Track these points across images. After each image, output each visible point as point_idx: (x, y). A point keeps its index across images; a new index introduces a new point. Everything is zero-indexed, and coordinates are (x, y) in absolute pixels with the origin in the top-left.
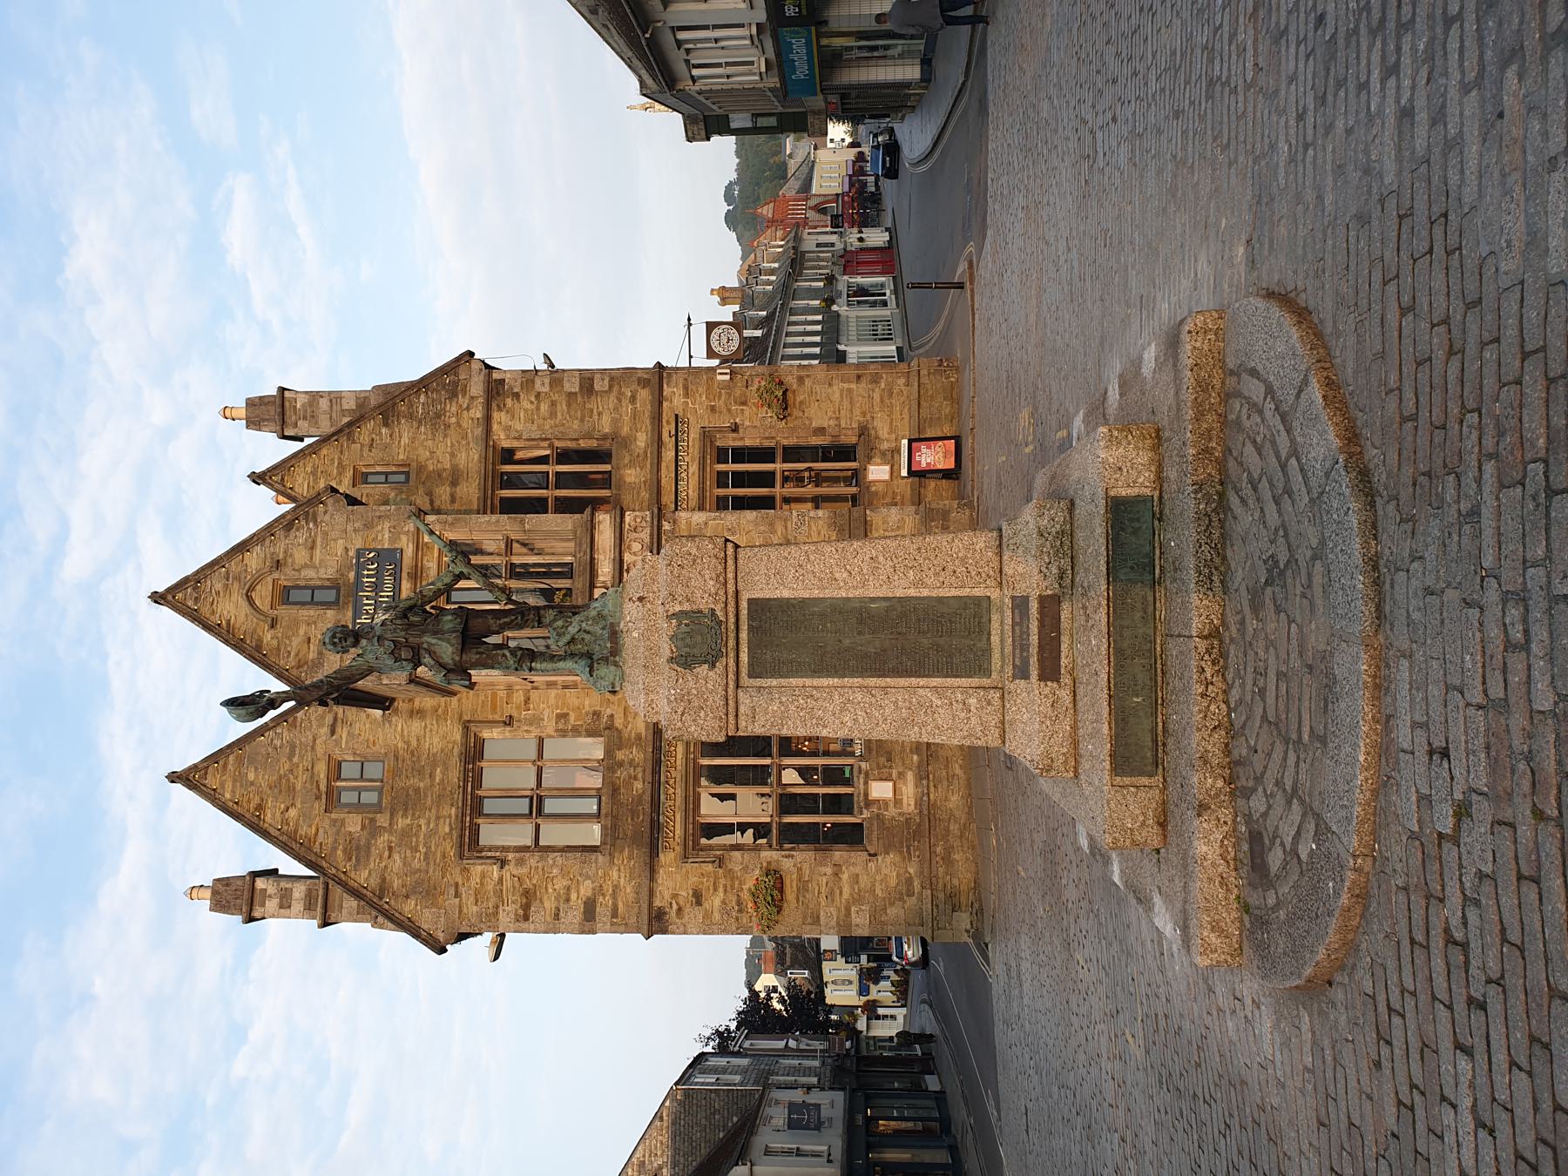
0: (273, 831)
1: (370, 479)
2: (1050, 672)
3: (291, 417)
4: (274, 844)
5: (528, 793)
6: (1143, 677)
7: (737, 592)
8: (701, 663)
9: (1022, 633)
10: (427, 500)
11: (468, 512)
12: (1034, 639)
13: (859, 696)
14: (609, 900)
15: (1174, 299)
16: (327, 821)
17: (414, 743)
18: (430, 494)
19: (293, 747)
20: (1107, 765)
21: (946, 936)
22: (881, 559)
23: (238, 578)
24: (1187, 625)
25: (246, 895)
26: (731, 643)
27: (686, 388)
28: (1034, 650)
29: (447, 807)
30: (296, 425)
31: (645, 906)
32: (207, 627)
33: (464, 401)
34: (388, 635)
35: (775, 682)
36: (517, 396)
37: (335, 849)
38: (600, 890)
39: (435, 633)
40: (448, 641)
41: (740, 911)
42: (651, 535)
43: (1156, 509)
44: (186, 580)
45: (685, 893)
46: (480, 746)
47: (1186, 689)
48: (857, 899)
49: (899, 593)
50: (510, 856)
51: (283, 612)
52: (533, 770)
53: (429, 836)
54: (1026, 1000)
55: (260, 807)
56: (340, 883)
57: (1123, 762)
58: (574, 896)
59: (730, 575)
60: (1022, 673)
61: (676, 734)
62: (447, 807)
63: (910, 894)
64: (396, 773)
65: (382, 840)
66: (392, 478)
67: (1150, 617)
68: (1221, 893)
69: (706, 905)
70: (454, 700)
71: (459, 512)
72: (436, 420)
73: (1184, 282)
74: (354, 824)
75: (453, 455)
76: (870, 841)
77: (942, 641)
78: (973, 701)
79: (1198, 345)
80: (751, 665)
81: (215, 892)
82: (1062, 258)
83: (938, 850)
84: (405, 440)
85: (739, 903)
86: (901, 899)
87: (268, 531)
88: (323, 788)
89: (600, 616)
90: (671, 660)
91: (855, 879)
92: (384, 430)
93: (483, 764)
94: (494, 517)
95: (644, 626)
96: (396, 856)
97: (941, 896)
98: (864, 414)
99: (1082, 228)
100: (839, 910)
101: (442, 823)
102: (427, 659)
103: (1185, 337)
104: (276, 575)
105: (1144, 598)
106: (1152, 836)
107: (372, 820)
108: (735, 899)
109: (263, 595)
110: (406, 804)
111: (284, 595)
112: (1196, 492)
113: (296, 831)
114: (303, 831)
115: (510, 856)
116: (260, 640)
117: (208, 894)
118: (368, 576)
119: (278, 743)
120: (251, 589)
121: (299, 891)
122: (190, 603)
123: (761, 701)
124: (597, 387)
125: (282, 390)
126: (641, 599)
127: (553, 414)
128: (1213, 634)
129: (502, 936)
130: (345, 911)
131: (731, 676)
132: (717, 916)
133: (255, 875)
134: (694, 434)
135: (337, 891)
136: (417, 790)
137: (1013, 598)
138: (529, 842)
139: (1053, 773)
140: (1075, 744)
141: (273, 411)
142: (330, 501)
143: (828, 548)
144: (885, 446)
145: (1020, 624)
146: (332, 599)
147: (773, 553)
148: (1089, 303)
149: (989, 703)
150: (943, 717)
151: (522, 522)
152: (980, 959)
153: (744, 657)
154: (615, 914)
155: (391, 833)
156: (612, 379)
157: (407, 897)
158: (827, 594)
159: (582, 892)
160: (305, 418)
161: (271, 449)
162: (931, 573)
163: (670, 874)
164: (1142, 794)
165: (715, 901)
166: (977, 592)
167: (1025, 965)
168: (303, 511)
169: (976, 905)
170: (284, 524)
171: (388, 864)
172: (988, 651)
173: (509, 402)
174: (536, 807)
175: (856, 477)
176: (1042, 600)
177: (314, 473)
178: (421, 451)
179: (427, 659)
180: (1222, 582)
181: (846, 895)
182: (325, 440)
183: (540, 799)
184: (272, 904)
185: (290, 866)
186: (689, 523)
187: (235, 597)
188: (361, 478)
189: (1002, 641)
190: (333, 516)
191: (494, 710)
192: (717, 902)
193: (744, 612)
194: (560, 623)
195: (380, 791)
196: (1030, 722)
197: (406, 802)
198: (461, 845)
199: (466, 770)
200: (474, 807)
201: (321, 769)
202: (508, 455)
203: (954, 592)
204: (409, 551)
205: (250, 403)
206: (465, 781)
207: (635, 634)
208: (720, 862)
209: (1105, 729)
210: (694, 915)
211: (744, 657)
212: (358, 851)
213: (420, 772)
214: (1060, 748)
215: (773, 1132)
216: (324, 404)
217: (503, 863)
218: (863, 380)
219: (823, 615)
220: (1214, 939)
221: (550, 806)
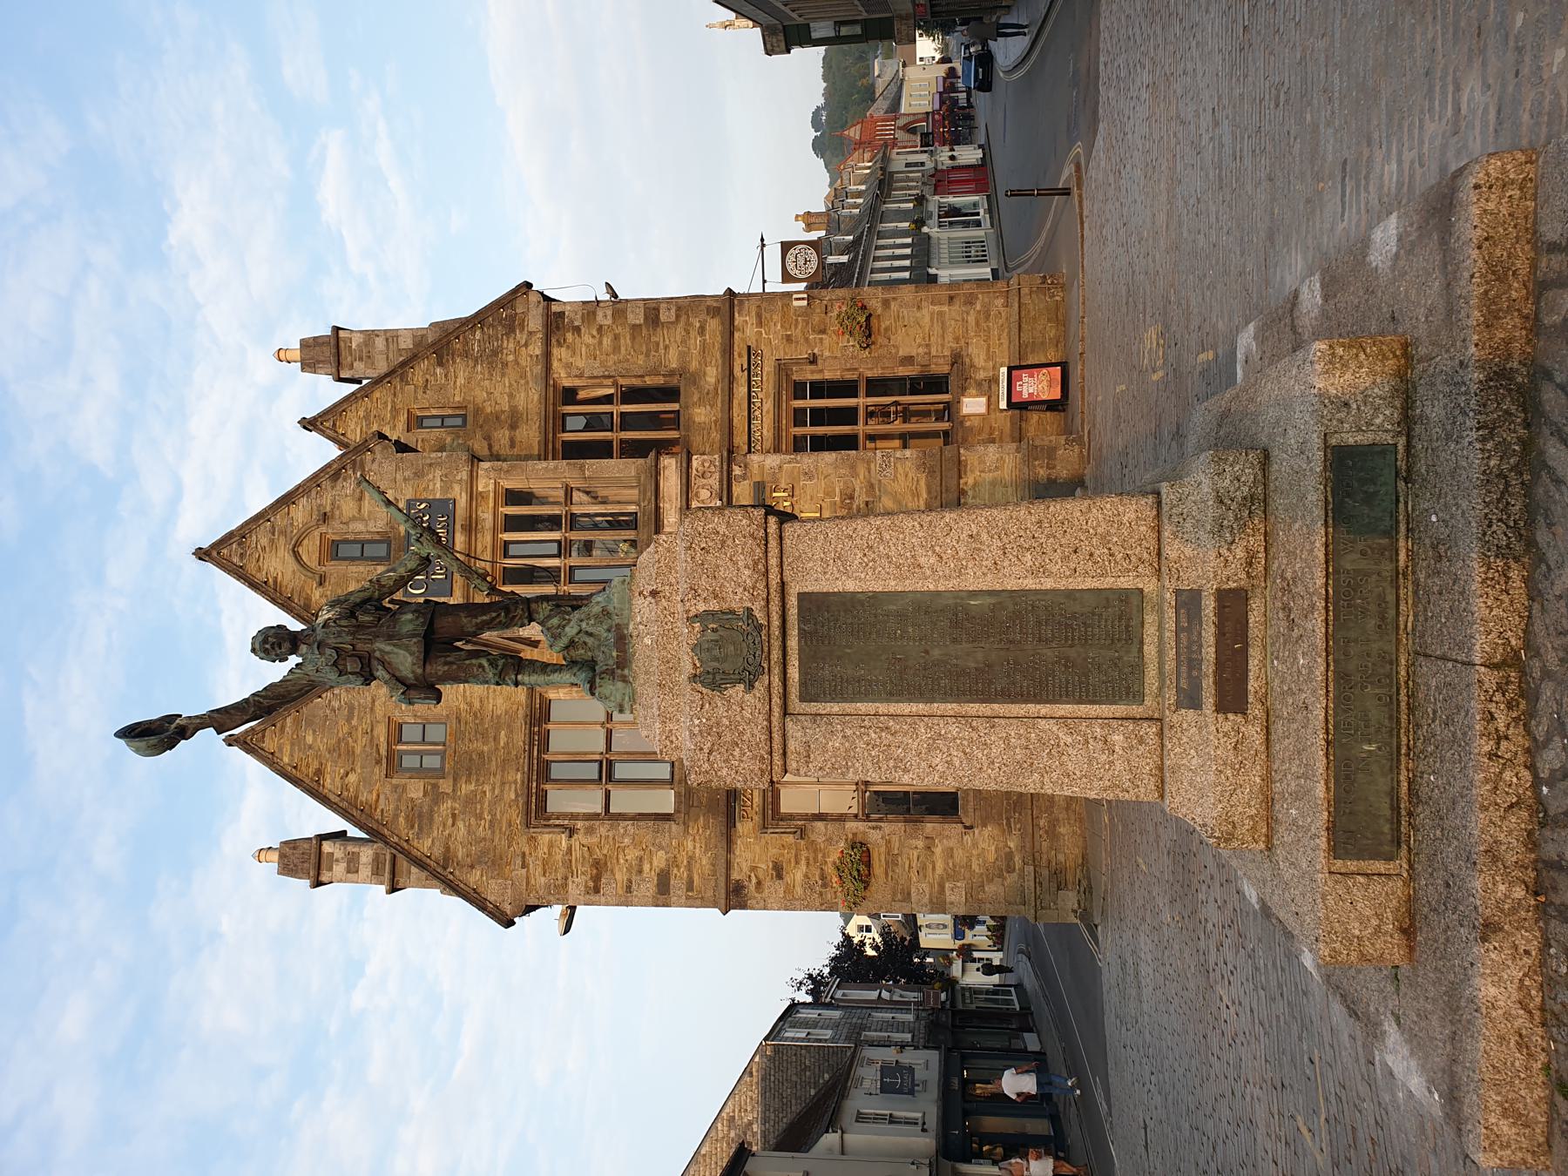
0: (333, 798)
1: (426, 423)
2: (1232, 699)
3: (346, 359)
4: (335, 810)
5: (598, 757)
6: (1377, 714)
7: (783, 584)
8: (734, 683)
9: (1190, 643)
10: (485, 444)
11: (528, 458)
12: (1209, 653)
13: (954, 730)
15: (1408, 156)
16: (388, 786)
17: (477, 704)
18: (488, 438)
19: (351, 709)
20: (1322, 842)
21: (1050, 916)
22: (985, 536)
23: (283, 533)
24: (1465, 644)
25: (313, 860)
26: (776, 655)
27: (759, 316)
28: (1209, 668)
29: (512, 773)
30: (351, 367)
31: (723, 879)
32: (253, 585)
33: (521, 337)
34: (332, 641)
35: (836, 708)
37: (396, 816)
38: (674, 862)
39: (390, 638)
40: (407, 648)
41: (824, 885)
43: (1402, 464)
44: (231, 535)
45: (765, 866)
46: (546, 706)
47: (1460, 742)
48: (951, 874)
49: (1011, 585)
50: (580, 824)
52: (602, 733)
53: (493, 803)
54: (1145, 1007)
55: (319, 772)
56: (403, 852)
57: (1347, 837)
58: (646, 867)
59: (773, 561)
60: (1190, 700)
61: (702, 779)
62: (512, 773)
63: (1011, 870)
64: (458, 736)
65: (445, 807)
66: (448, 422)
67: (1388, 625)
68: (1519, 1060)
69: (788, 879)
71: (519, 458)
72: (493, 357)
73: (1431, 127)
74: (416, 790)
75: (511, 396)
76: (966, 812)
77: (1072, 653)
78: (1117, 738)
79: (1491, 206)
80: (803, 684)
81: (282, 856)
82: (1206, 137)
83: (1042, 823)
84: (461, 381)
85: (823, 877)
86: (1001, 876)
87: (314, 482)
88: (383, 752)
89: (606, 613)
90: (694, 678)
91: (949, 853)
92: (438, 370)
93: (549, 726)
94: (552, 464)
95: (660, 629)
96: (460, 824)
97: (1045, 872)
98: (957, 339)
99: (1237, 92)
100: (932, 886)
101: (508, 789)
102: (380, 673)
103: (1467, 195)
104: (323, 529)
105: (1382, 598)
106: (1392, 948)
107: (435, 786)
108: (818, 873)
109: (310, 551)
110: (469, 769)
111: (333, 550)
112: (1483, 440)
113: (356, 797)
114: (363, 797)
115: (580, 824)
116: (308, 599)
117: (275, 856)
119: (336, 704)
120: (298, 543)
121: (366, 854)
122: (235, 560)
123: (817, 733)
124: (663, 318)
125: (337, 329)
126: (654, 594)
127: (616, 349)
128: (1509, 662)
129: (573, 909)
130: (413, 877)
131: (776, 700)
132: (799, 890)
133: (322, 838)
134: (769, 367)
135: (402, 862)
136: (481, 754)
137: (1177, 592)
138: (598, 808)
139: (1235, 844)
140: (1269, 802)
141: (328, 352)
142: (378, 449)
143: (908, 523)
144: (981, 375)
145: (1189, 630)
146: (383, 553)
147: (832, 530)
148: (1249, 188)
149: (1141, 741)
150: (1075, 761)
151: (582, 468)
152: (1086, 935)
153: (794, 673)
154: (690, 887)
155: (454, 799)
156: (679, 309)
157: (472, 867)
158: (908, 585)
159: (655, 863)
160: (361, 359)
162: (1057, 556)
163: (748, 845)
164: (1376, 887)
165: (797, 875)
166: (1125, 582)
167: (1145, 970)
168: (352, 457)
169: (1084, 883)
170: (331, 473)
171: (452, 833)
172: (1139, 667)
173: (569, 336)
174: (606, 773)
175: (948, 411)
176: (1221, 595)
177: (367, 417)
178: (477, 392)
179: (380, 673)
180: (1525, 580)
181: (939, 871)
182: (377, 382)
183: (610, 763)
184: (339, 869)
185: (353, 832)
186: (761, 467)
187: (281, 552)
188: (416, 422)
189: (1161, 653)
190: (382, 466)
192: (799, 876)
193: (793, 612)
194: (555, 621)
195: (443, 754)
196: (1200, 770)
197: (471, 766)
198: (528, 813)
199: (531, 734)
200: (541, 772)
201: (381, 733)
202: (570, 395)
203: (1090, 584)
204: (462, 502)
205: (304, 344)
206: (531, 745)
207: (647, 641)
208: (802, 833)
209: (1320, 790)
210: (774, 889)
211: (794, 673)
212: (421, 818)
213: (484, 735)
214: (1247, 807)
215: (864, 1097)
216: (380, 343)
217: (572, 832)
218: (957, 302)
219: (901, 616)
220: (1506, 1128)
221: (621, 771)
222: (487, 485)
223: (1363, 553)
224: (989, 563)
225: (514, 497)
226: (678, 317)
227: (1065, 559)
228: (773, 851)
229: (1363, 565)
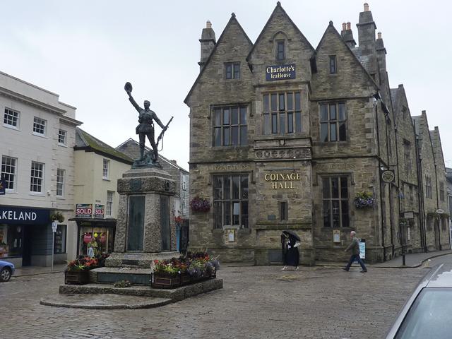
1: (332, 61)
27: (368, 166)
42: (279, 158)
44: (285, 12)
51: (275, 44)
65: (215, 81)
91: (205, 225)
96: (211, 86)
104: (286, 40)
109: (279, 37)
124: (367, 135)
127: (357, 120)
134: (350, 171)
175: (337, 225)
204: (294, 81)
217: (209, 118)
218: (372, 229)
226: (367, 139)
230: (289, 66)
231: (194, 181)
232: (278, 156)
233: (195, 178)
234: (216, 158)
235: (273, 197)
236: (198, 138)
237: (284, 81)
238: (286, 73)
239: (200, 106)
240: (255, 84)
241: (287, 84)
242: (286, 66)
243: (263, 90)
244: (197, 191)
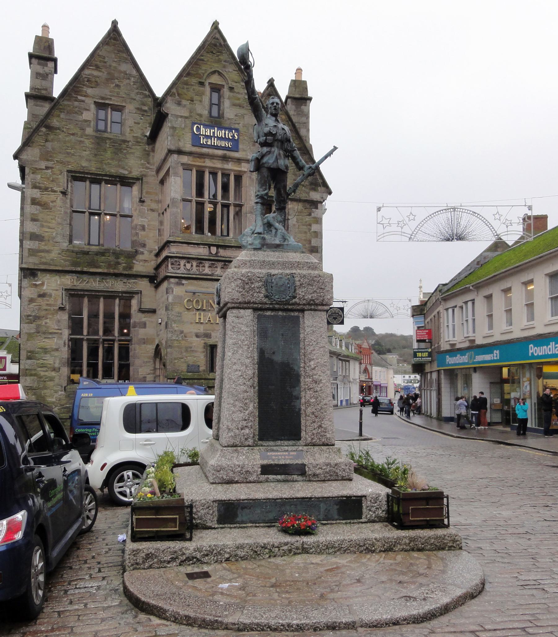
5: (102, 208)
14: (43, 247)
36: (310, 215)
69: (39, 299)
70: (154, 173)
101: (86, 161)
118: (225, 134)
120: (220, 74)
125: (310, 99)
161: (283, 91)
162: (314, 410)
163: (56, 281)
191: (147, 193)
193: (292, 314)
208: (62, 309)
222: (244, 167)
223: (326, 509)
224: (311, 387)
225: (238, 178)
227: (313, 413)
228: (53, 293)
229: (322, 510)
230: (230, 129)
231: (31, 300)
232: (207, 271)
233: (35, 296)
234: (75, 264)
235: (197, 336)
236: (42, 226)
237: (220, 152)
238: (225, 139)
239: (47, 168)
240: (173, 148)
241: (225, 158)
242: (226, 129)
243: (185, 159)
244: (37, 318)
